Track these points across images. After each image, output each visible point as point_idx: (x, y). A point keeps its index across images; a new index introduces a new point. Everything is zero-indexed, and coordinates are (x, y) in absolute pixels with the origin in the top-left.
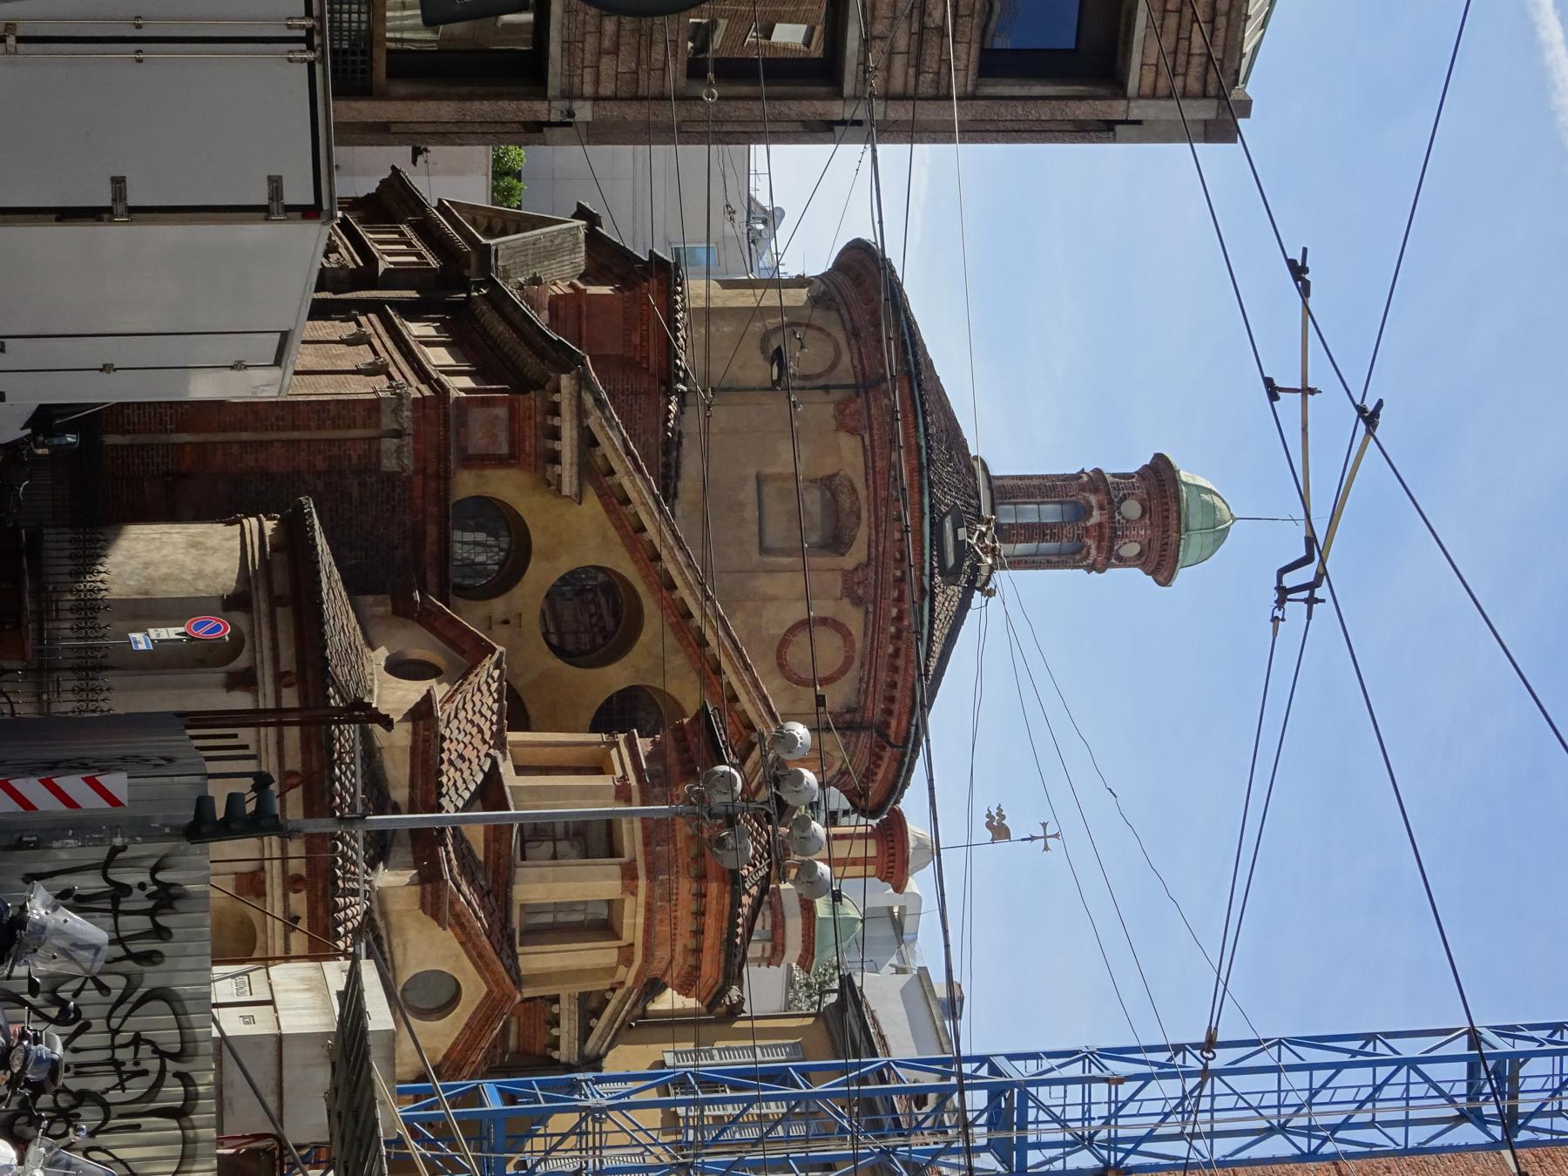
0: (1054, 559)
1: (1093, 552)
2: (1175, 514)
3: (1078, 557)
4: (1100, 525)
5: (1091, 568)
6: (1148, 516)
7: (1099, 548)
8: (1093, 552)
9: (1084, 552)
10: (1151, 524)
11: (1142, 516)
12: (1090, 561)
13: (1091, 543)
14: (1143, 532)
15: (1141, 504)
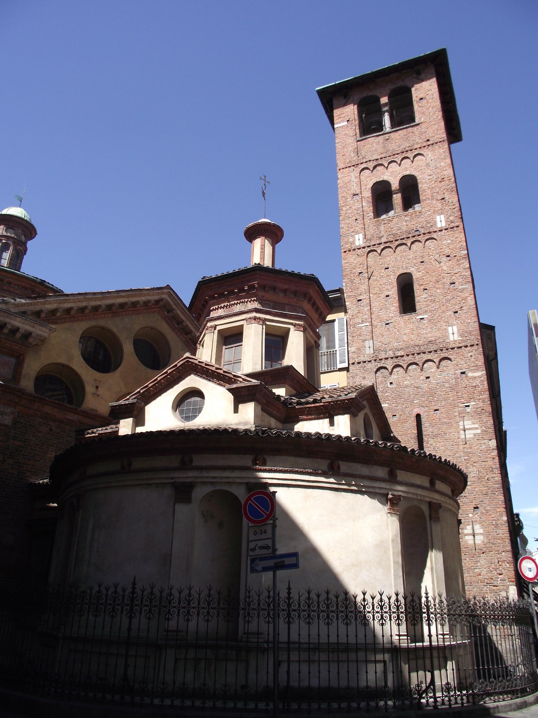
0: (19, 261)
1: (21, 248)
2: (17, 219)
3: (21, 254)
4: (14, 243)
5: (25, 254)
6: (14, 228)
7: (21, 246)
8: (21, 248)
9: (19, 251)
10: (18, 228)
11: (14, 229)
12: (23, 252)
13: (19, 247)
14: (19, 231)
15: (10, 228)
